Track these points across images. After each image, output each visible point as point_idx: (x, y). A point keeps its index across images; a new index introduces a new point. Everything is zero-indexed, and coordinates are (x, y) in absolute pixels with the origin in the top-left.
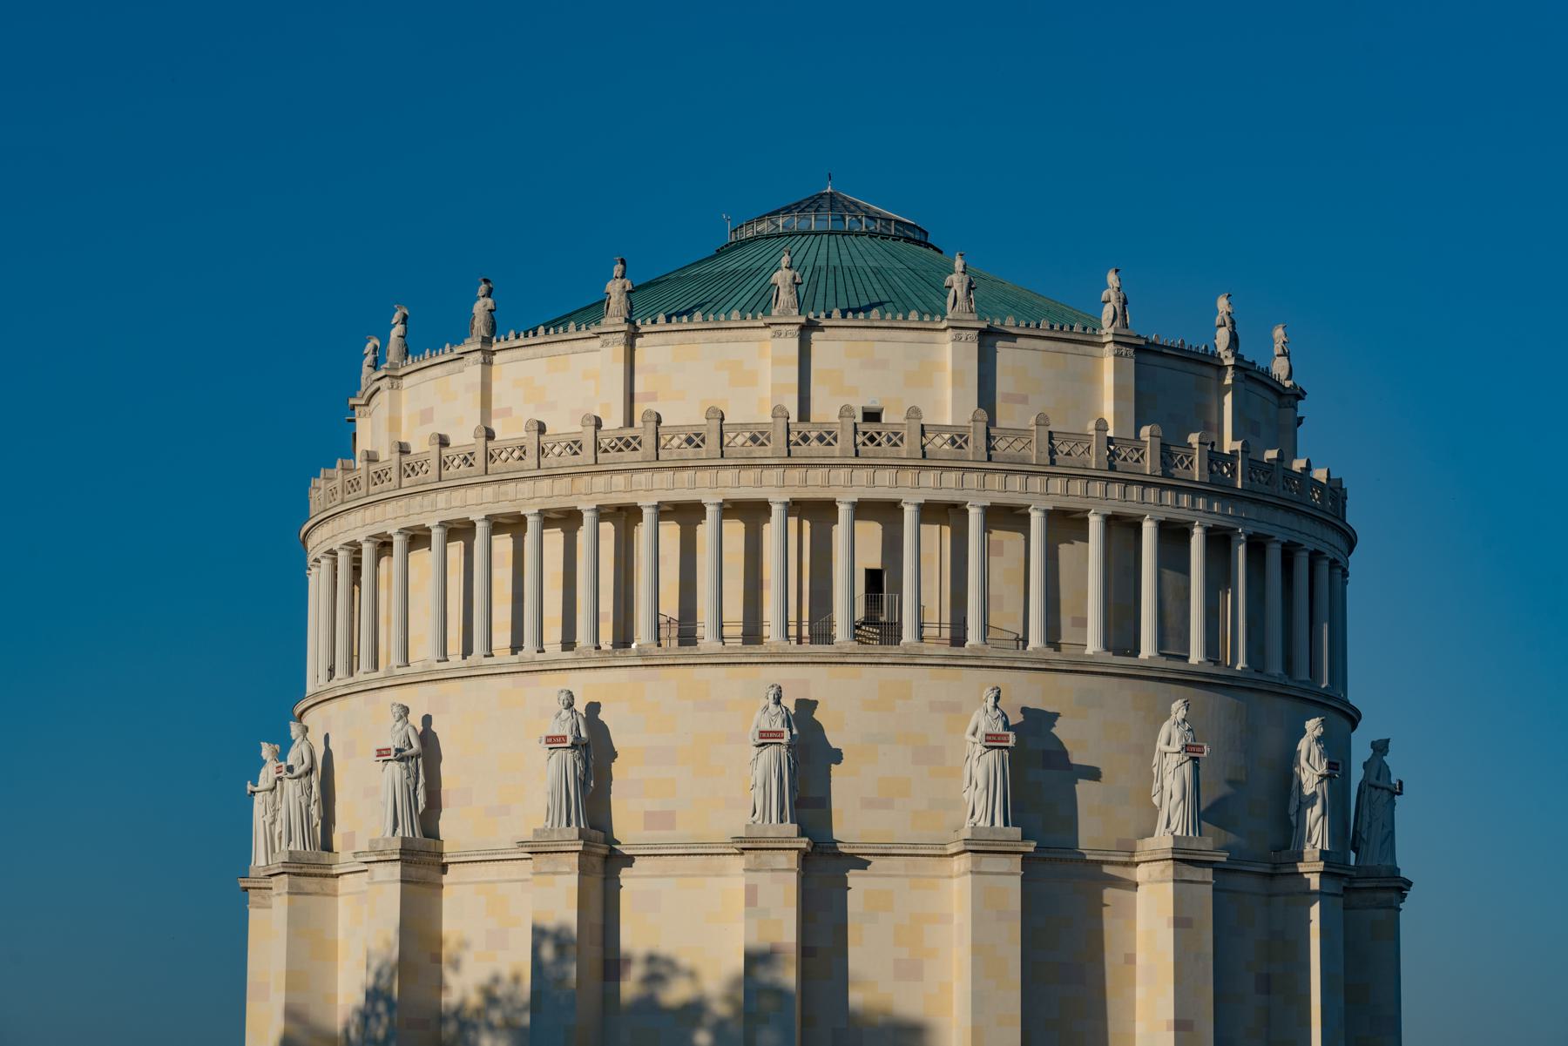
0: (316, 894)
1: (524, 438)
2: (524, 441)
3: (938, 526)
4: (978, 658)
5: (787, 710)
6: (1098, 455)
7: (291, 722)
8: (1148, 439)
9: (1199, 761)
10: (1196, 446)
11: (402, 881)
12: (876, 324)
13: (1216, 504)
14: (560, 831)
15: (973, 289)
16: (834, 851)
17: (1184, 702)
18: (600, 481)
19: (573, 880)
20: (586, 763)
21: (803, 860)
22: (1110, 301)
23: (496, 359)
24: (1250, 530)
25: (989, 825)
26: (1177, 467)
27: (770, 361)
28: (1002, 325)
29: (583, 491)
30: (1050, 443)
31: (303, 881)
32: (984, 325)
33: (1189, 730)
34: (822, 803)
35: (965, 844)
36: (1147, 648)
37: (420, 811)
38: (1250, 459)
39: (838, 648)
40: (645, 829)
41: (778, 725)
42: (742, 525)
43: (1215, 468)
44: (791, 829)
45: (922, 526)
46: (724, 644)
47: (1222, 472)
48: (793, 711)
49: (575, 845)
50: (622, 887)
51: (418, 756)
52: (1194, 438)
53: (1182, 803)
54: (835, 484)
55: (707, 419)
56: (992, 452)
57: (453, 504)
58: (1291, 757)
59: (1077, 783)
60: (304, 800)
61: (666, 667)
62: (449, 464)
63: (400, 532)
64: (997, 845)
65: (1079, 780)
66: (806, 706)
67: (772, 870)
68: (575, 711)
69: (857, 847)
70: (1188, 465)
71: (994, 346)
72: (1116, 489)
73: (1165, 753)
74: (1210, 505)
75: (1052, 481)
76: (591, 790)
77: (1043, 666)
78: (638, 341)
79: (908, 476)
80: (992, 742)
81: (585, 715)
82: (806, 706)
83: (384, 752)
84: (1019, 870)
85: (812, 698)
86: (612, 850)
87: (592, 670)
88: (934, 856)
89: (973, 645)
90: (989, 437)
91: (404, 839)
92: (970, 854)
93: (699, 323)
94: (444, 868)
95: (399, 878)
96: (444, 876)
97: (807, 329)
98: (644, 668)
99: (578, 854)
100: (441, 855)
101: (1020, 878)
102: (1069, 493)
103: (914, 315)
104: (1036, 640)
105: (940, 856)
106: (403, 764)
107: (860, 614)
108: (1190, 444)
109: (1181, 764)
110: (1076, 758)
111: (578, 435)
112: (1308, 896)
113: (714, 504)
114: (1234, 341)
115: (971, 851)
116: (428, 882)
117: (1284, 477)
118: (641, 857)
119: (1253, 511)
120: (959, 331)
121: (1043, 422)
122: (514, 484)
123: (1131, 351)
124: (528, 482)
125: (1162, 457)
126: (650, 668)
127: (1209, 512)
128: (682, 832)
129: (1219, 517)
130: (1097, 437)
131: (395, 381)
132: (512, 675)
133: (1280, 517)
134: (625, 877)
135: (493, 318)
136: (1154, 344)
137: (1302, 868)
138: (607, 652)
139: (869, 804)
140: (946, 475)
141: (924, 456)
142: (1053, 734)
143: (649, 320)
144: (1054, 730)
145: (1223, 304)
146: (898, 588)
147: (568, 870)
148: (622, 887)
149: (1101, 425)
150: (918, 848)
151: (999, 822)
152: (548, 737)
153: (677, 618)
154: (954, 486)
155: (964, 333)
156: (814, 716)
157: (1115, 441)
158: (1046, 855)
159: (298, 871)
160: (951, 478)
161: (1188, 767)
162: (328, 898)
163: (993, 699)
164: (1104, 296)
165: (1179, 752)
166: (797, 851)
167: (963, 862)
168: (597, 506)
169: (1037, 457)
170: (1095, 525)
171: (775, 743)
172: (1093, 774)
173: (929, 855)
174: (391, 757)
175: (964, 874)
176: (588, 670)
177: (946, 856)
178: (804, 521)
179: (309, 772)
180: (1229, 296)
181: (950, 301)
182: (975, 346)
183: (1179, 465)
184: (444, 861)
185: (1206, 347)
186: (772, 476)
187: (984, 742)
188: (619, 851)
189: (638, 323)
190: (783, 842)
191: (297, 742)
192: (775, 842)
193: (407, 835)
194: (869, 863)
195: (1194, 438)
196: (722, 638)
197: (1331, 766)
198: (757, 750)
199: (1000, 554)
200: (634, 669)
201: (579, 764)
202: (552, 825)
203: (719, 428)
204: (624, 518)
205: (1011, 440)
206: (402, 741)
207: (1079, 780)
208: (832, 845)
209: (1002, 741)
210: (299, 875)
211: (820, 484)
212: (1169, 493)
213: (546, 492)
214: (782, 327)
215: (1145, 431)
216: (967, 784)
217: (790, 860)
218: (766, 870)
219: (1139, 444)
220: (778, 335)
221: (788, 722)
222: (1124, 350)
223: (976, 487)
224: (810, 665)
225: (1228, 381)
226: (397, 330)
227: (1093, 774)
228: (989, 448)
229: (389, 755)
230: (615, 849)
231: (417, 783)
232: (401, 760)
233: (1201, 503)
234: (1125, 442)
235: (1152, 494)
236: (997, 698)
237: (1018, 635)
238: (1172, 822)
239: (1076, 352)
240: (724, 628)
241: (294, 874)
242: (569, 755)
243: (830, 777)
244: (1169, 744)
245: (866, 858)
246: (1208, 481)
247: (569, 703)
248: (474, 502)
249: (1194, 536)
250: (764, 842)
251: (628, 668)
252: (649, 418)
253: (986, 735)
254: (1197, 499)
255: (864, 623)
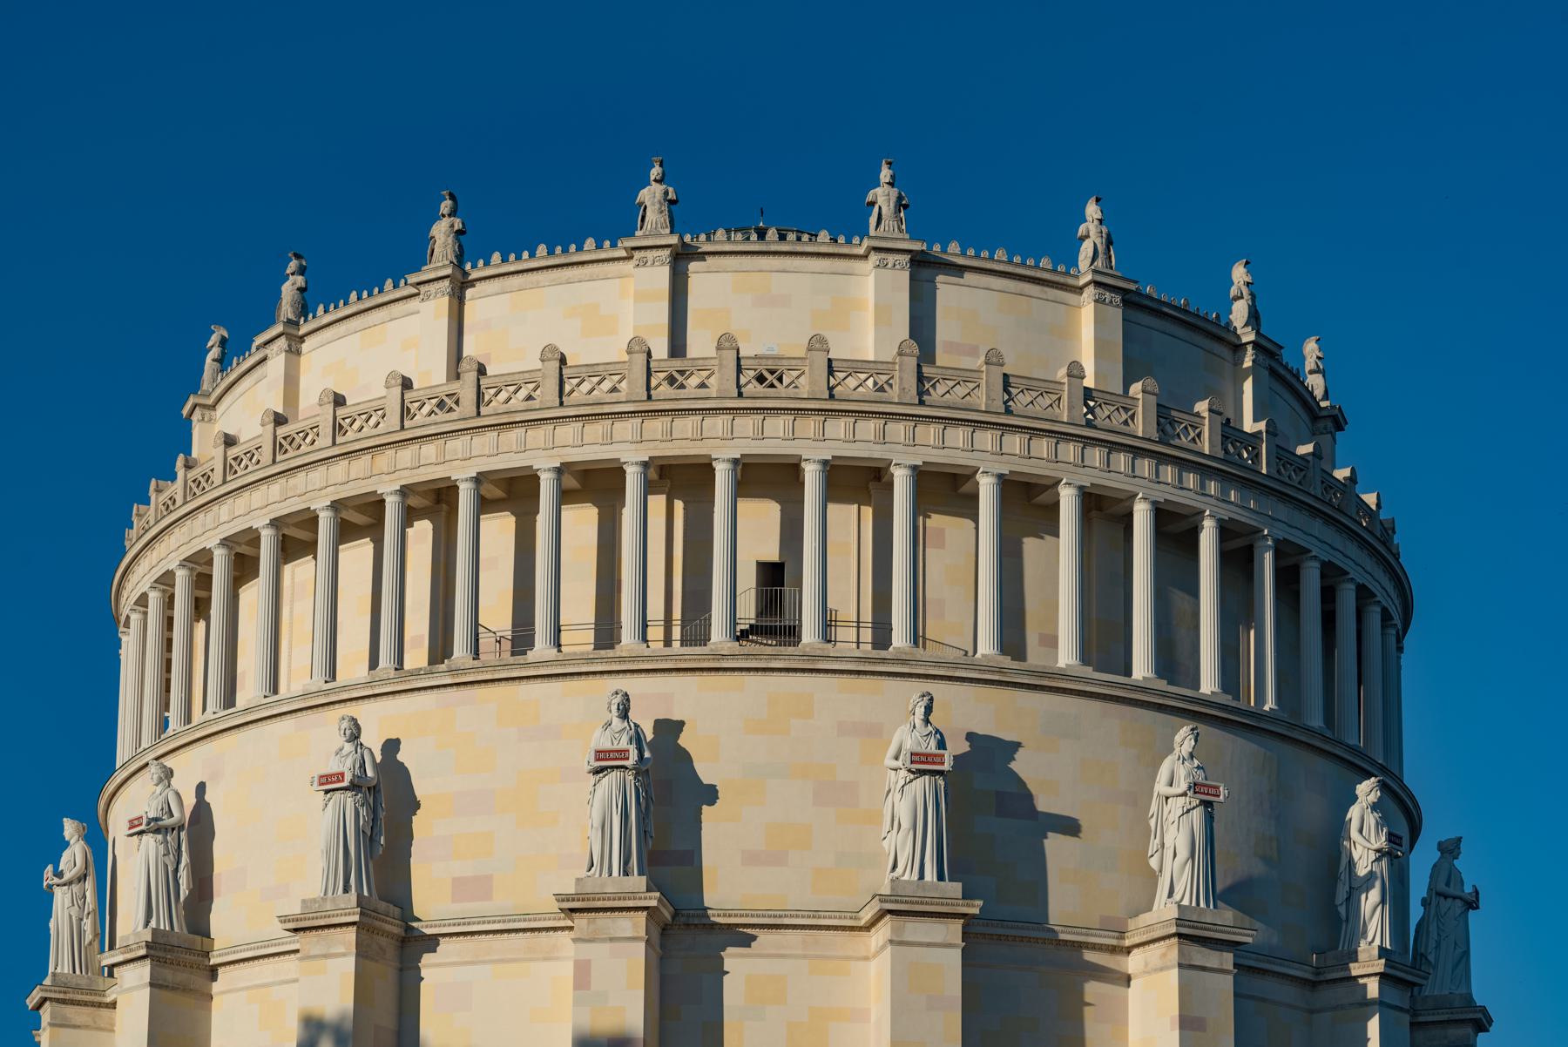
0: (87, 1027)
1: (318, 415)
2: (318, 419)
3: (856, 506)
4: (904, 662)
5: (637, 726)
6: (1071, 408)
7: (65, 819)
8: (1140, 396)
9: (1213, 809)
10: (1206, 414)
11: (152, 985)
12: (773, 248)
13: (1233, 492)
14: (334, 900)
15: (906, 207)
16: (704, 921)
17: (1193, 730)
18: (406, 455)
19: (349, 964)
20: (374, 811)
21: (662, 934)
22: (1088, 236)
23: (305, 347)
24: (1281, 535)
25: (916, 878)
26: (1180, 438)
27: (632, 301)
28: (944, 251)
29: (385, 470)
30: (1006, 390)
31: (70, 1011)
32: (917, 246)
33: (1198, 767)
34: (690, 858)
35: (881, 901)
36: (1142, 666)
37: (182, 899)
38: (1277, 446)
39: (712, 650)
40: (454, 901)
41: (623, 744)
42: (596, 510)
43: (1231, 449)
44: (638, 882)
45: (831, 507)
46: (559, 651)
47: (1240, 456)
48: (649, 736)
49: (349, 914)
50: (423, 979)
51: (181, 828)
52: (1202, 407)
53: (1190, 861)
54: (709, 436)
55: (542, 361)
56: (925, 398)
57: (236, 515)
58: (1338, 828)
59: (1046, 838)
60: (74, 912)
61: (483, 686)
62: (237, 468)
63: (181, 565)
64: (927, 904)
65: (1050, 834)
66: (669, 729)
67: (611, 940)
68: (361, 744)
69: (736, 916)
70: (1194, 439)
71: (933, 282)
72: (1096, 455)
73: (1167, 798)
74: (1225, 492)
75: (1007, 438)
76: (381, 849)
77: (996, 677)
78: (469, 293)
79: (809, 425)
80: (921, 765)
81: (379, 758)
82: (669, 729)
83: (136, 822)
84: (958, 940)
85: (675, 718)
86: (409, 929)
87: (391, 697)
88: (843, 928)
89: (899, 648)
90: (921, 378)
91: (155, 932)
92: (888, 916)
93: (543, 257)
94: (213, 973)
95: (147, 979)
96: (213, 983)
97: (681, 258)
98: (455, 688)
99: (355, 928)
100: (207, 955)
101: (959, 951)
102: (1032, 455)
103: (824, 236)
104: (987, 646)
105: (852, 928)
106: (160, 837)
107: (748, 611)
108: (1198, 415)
109: (1188, 811)
110: (1043, 804)
111: (380, 402)
112: (1366, 1006)
113: (549, 470)
114: (1254, 318)
115: (890, 912)
116: (191, 990)
117: (1323, 482)
118: (447, 939)
119: (1282, 511)
120: (883, 255)
121: (994, 360)
122: (304, 473)
123: (1118, 299)
124: (320, 468)
125: (1158, 424)
126: (462, 688)
127: (1224, 501)
128: (502, 902)
129: (1239, 511)
130: (1069, 385)
131: (207, 412)
132: (294, 715)
133: (1317, 527)
134: (425, 966)
135: (303, 299)
136: (1149, 297)
137: (1355, 970)
138: (409, 671)
139: (752, 859)
140: (861, 424)
141: (832, 397)
142: (1010, 769)
143: (481, 263)
144: (1013, 765)
145: (1239, 274)
146: (799, 583)
147: (342, 950)
148: (423, 979)
149: (1076, 372)
150: (819, 917)
151: (930, 874)
152: (322, 777)
153: (509, 634)
154: (872, 438)
155: (891, 258)
156: (679, 742)
157: (1095, 394)
158: (1000, 931)
159: (61, 996)
160: (868, 428)
161: (1197, 815)
162: (105, 1034)
163: (923, 709)
164: (1082, 230)
165: (1185, 794)
166: (645, 913)
167: (884, 930)
168: (401, 487)
169: (986, 404)
170: (1068, 501)
171: (617, 767)
172: (1070, 827)
173: (836, 928)
174: (143, 827)
175: (883, 948)
176: (385, 698)
177: (860, 929)
178: (676, 501)
179: (82, 878)
180: (1247, 263)
181: (873, 220)
182: (907, 274)
183: (1182, 436)
184: (211, 963)
185: (1218, 316)
186: (625, 428)
187: (908, 764)
188: (417, 929)
189: (468, 266)
190: (625, 899)
191: (72, 842)
192: (614, 899)
193: (162, 928)
194: (754, 938)
195: (1202, 407)
196: (559, 645)
197: (1393, 838)
198: (592, 779)
199: (941, 545)
200: (442, 690)
201: (363, 812)
202: (325, 895)
203: (558, 371)
204: (444, 514)
205: (951, 383)
206: (160, 808)
207: (1050, 834)
208: (703, 912)
209: (934, 763)
210: (63, 1002)
211: (690, 436)
212: (1169, 468)
213: (341, 478)
214: (650, 254)
215: (1136, 389)
216: (887, 826)
217: (636, 925)
218: (603, 940)
219: (1129, 401)
220: (643, 263)
221: (638, 738)
222: (1108, 295)
223: (903, 440)
224: (674, 674)
225: (1248, 363)
226: (214, 353)
227: (1070, 827)
228: (921, 393)
229: (141, 824)
230: (413, 928)
231: (178, 863)
232: (157, 831)
233: (1212, 487)
234: (1108, 397)
235: (1145, 466)
236: (929, 709)
237: (966, 652)
238: (1176, 890)
239: (1045, 297)
240: (562, 632)
241: (58, 1001)
242: (349, 800)
243: (701, 822)
244: (1171, 785)
245: (749, 931)
246: (1222, 457)
247: (352, 733)
248: (260, 505)
249: (1204, 530)
250: (599, 900)
251: (435, 691)
252: (468, 367)
253: (912, 754)
254: (1207, 482)
255: (753, 629)
